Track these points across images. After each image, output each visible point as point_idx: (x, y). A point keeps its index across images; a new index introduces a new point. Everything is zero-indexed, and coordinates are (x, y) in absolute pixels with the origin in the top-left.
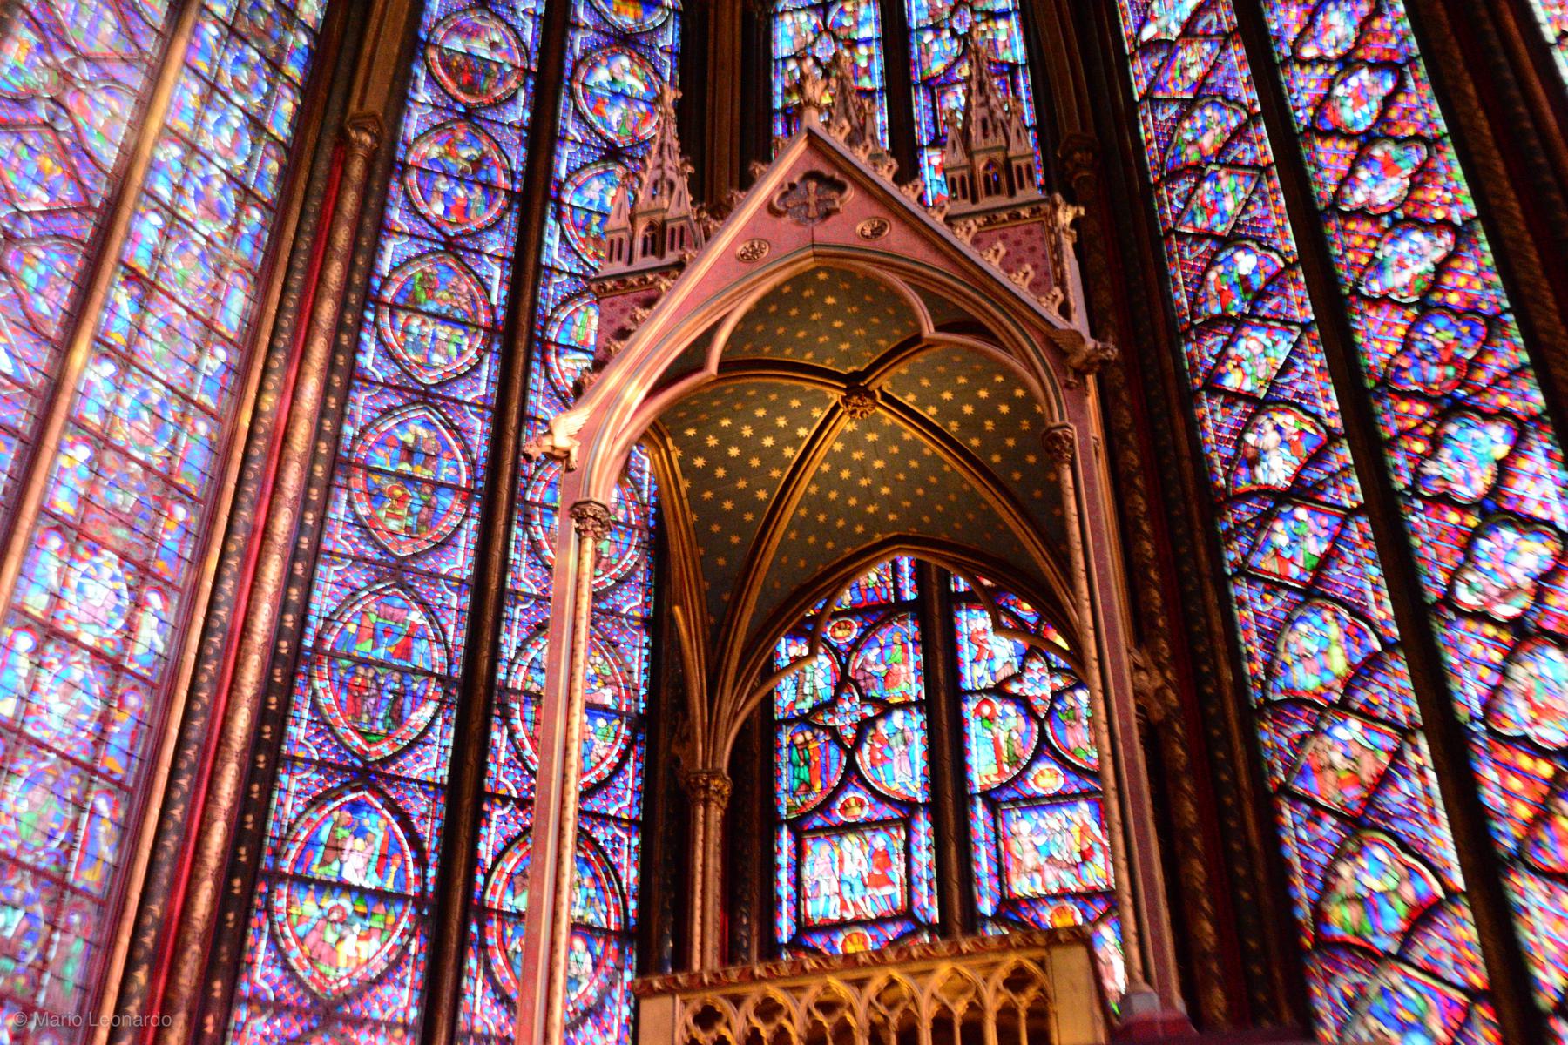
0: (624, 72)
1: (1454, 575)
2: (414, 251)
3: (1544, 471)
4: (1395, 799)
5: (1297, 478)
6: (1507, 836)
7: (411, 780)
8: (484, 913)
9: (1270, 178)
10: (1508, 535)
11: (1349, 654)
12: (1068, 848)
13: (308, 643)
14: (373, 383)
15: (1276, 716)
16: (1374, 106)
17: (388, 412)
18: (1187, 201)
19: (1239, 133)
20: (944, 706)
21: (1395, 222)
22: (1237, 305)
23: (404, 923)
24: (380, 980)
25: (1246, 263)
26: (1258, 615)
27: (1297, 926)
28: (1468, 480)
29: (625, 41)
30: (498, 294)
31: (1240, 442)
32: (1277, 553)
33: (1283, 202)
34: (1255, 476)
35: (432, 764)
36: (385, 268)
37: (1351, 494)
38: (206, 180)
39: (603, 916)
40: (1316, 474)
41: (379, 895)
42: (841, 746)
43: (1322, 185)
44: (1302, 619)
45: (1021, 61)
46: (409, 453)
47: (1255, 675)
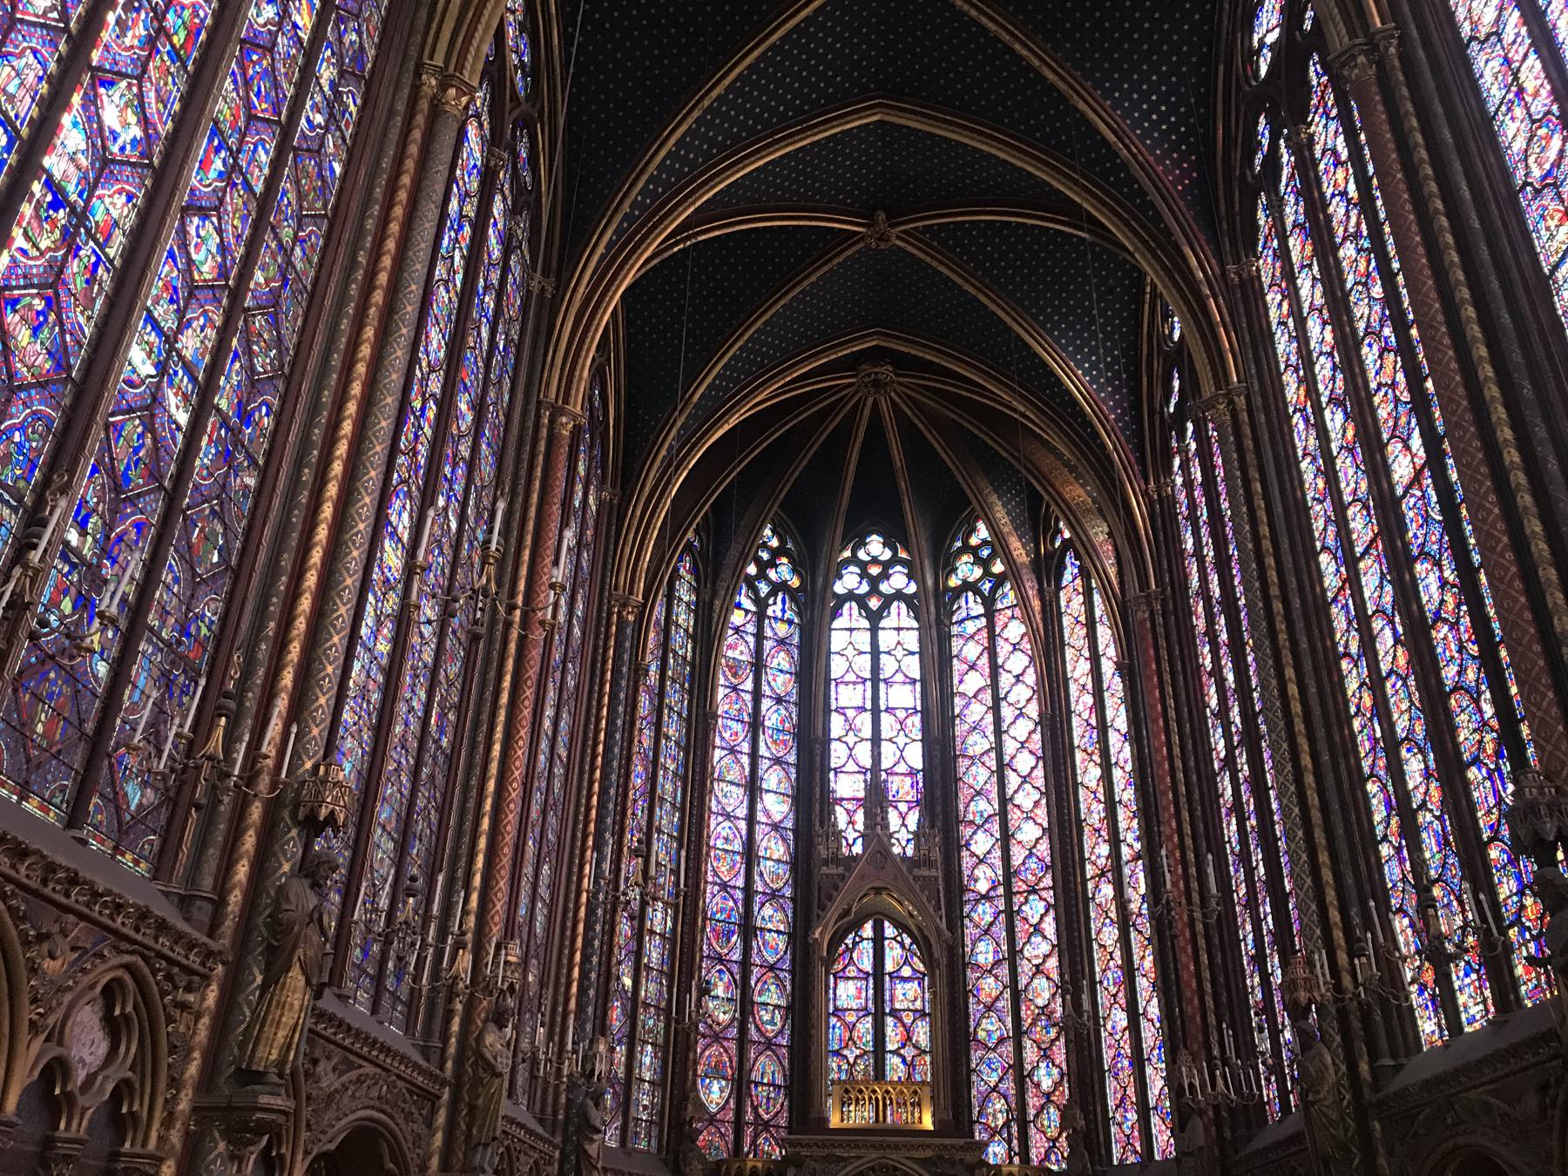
4: (1000, 1004)
6: (1026, 1025)
10: (1040, 939)
12: (911, 995)
20: (879, 941)
22: (978, 821)
35: (736, 956)
39: (783, 1002)
46: (726, 839)
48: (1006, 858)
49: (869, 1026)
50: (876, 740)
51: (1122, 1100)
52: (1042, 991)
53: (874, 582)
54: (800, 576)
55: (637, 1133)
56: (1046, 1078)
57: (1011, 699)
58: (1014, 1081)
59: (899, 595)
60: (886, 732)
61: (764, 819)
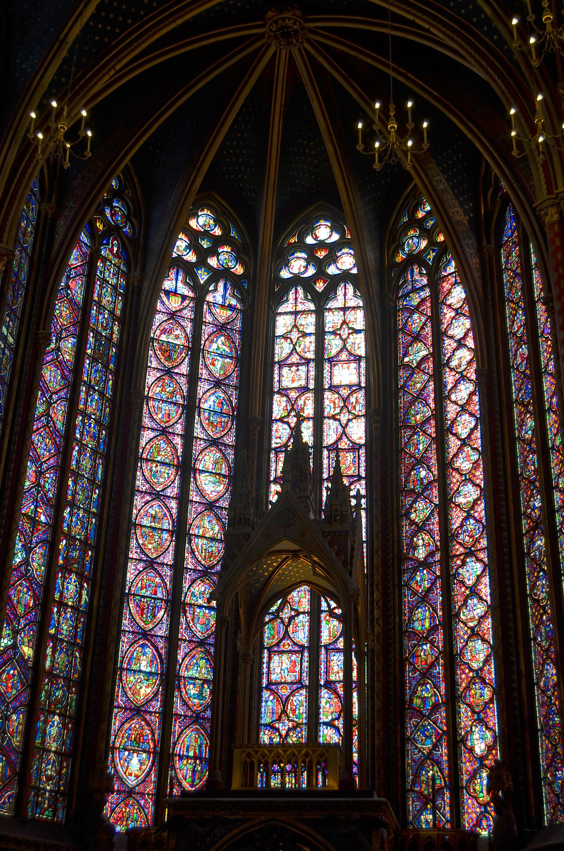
0: (220, 344)
1: (460, 608)
2: (151, 434)
5: (425, 558)
7: (157, 636)
8: (179, 677)
10: (476, 601)
11: (430, 624)
13: (127, 591)
14: (142, 492)
15: (409, 636)
16: (468, 430)
17: (147, 503)
18: (409, 439)
19: (428, 420)
21: (466, 479)
22: (418, 489)
23: (158, 682)
24: (151, 700)
25: (423, 473)
26: (408, 601)
27: (404, 702)
29: (222, 328)
30: (180, 451)
31: (412, 540)
32: (417, 582)
36: (143, 443)
38: (90, 426)
40: (430, 560)
41: (150, 673)
42: (284, 624)
43: (448, 454)
45: (363, 356)
46: (154, 517)
47: (405, 620)
48: (445, 523)
49: (302, 698)
50: (319, 419)
51: (552, 760)
52: (478, 653)
53: (321, 265)
54: (243, 264)
55: (38, 804)
56: (480, 742)
57: (453, 364)
58: (448, 746)
59: (345, 277)
60: (329, 410)
61: (197, 499)
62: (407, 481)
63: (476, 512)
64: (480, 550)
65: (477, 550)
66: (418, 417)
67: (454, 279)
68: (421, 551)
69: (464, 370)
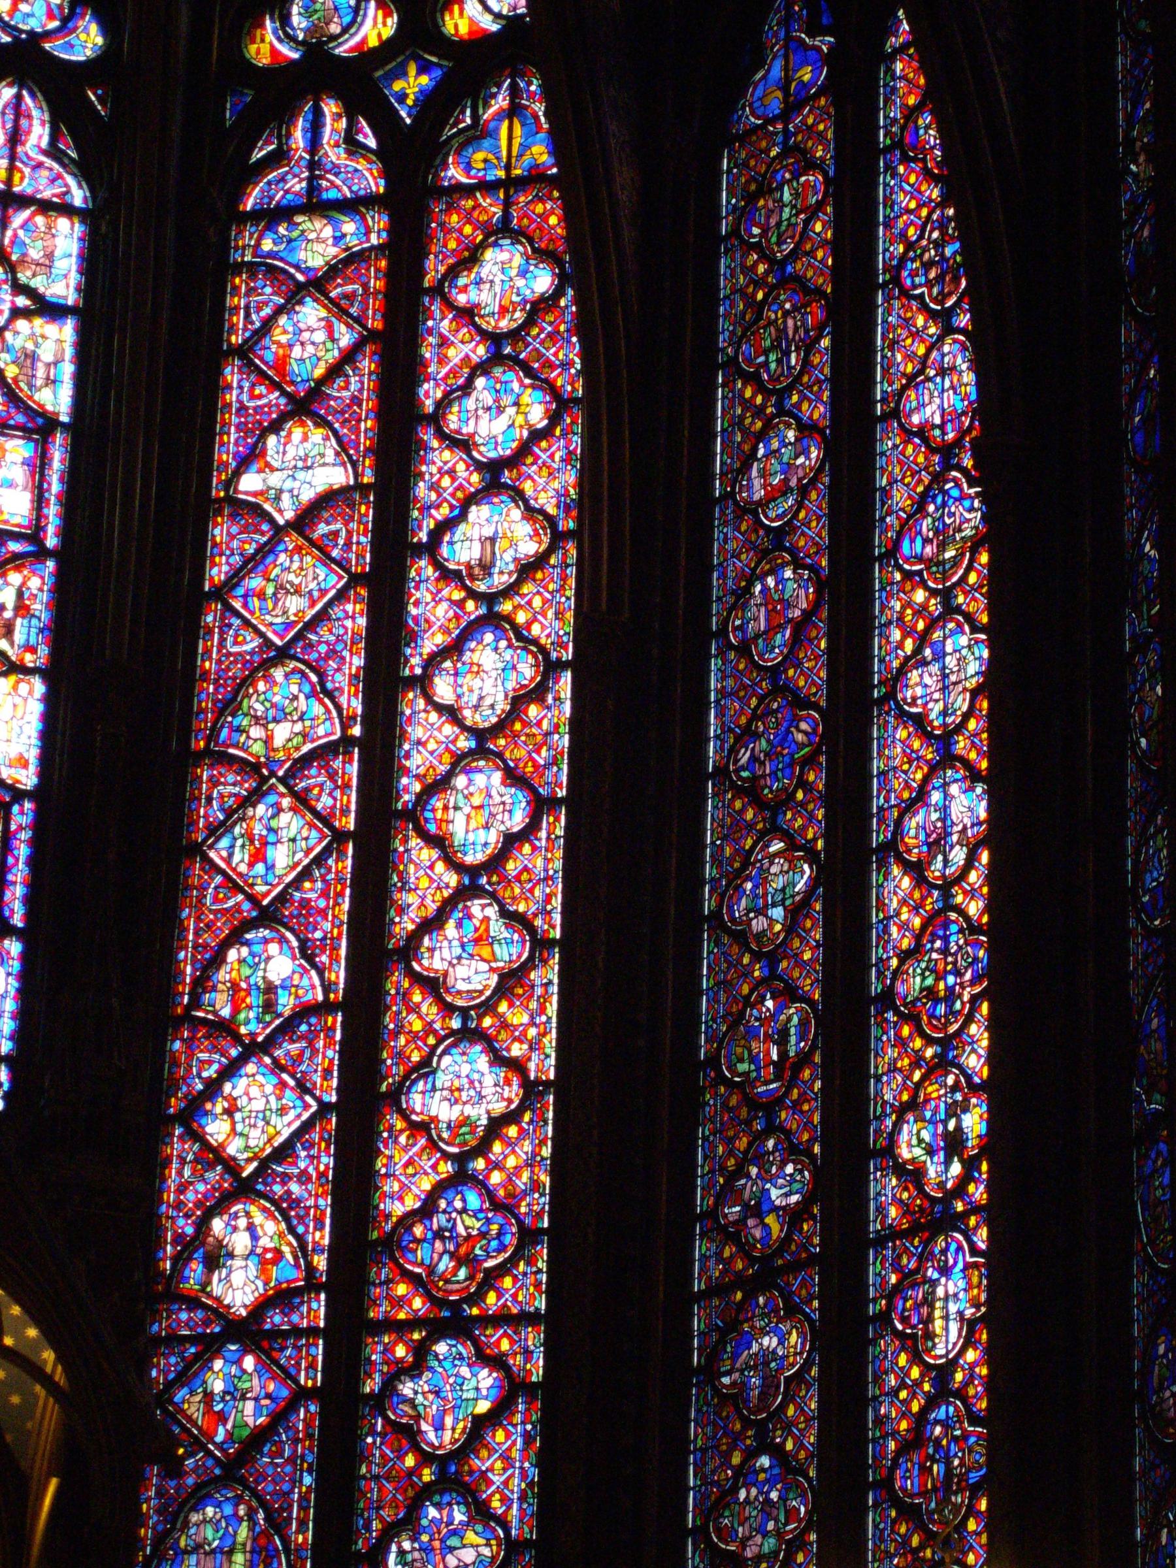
1: (390, 1532)
3: (515, 1454)
9: (341, 854)
10: (459, 1516)
18: (229, 813)
19: (323, 754)
22: (250, 1024)
25: (280, 965)
28: (439, 1427)
32: (209, 1397)
33: (346, 906)
34: (209, 1283)
37: (311, 1365)
40: (276, 1319)
43: (401, 911)
44: (209, 1496)
45: (64, 419)
48: (355, 1184)
62: (202, 983)
63: (498, 1166)
64: (502, 1319)
65: (487, 1320)
66: (282, 733)
67: (497, 211)
68: (238, 1278)
69: (510, 591)
